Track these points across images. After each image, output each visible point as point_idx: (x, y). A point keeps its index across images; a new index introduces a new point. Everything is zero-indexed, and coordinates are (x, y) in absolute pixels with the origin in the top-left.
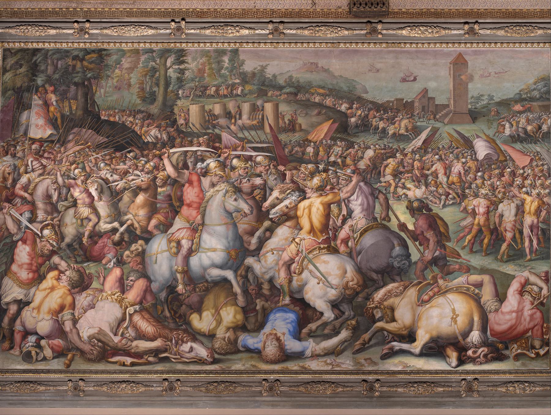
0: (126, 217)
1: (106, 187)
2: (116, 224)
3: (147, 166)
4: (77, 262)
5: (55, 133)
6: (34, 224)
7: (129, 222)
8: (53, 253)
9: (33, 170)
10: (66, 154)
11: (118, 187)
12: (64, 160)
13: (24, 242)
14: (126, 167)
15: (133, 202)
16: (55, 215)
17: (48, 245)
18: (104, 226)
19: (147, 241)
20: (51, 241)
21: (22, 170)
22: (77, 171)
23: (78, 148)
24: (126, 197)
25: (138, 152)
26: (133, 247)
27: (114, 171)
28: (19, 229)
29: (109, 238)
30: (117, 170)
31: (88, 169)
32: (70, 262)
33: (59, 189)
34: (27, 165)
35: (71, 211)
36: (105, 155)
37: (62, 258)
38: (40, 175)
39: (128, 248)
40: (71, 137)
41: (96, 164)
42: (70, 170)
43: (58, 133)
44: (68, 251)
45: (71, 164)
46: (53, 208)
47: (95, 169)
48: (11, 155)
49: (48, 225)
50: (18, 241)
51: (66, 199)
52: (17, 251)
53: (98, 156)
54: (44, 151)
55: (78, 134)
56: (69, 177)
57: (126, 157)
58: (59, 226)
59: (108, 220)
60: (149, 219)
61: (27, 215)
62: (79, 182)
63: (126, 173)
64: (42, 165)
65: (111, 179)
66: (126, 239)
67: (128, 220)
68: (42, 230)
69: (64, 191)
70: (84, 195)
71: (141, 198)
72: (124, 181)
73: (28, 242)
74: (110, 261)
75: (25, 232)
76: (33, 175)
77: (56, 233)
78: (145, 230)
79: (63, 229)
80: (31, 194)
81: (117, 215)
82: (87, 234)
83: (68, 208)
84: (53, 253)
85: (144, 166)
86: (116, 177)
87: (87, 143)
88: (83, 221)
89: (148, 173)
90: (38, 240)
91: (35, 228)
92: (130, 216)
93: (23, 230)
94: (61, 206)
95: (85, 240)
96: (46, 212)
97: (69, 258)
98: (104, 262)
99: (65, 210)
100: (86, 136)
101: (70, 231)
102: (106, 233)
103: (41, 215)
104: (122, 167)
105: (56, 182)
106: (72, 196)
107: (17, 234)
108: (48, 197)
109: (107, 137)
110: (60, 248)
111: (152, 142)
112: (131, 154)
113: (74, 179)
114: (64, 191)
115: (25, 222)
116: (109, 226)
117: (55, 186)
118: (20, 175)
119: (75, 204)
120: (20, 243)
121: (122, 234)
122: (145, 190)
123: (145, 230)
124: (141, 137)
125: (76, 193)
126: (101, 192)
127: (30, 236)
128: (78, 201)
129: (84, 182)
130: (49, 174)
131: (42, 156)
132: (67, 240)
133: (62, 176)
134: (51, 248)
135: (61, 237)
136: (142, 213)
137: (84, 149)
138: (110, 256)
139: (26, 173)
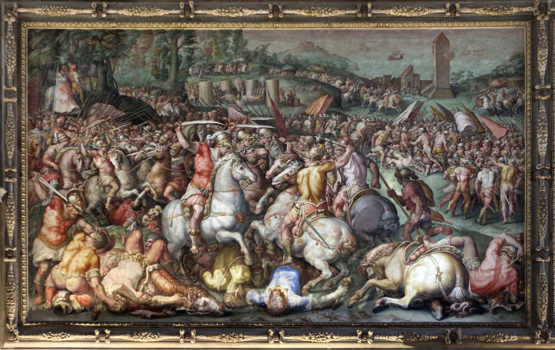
0: (144, 185)
2: (135, 191)
3: (162, 138)
4: (100, 225)
5: (78, 107)
6: (61, 191)
7: (147, 189)
8: (79, 217)
9: (59, 142)
10: (88, 127)
11: (136, 157)
12: (87, 132)
13: (53, 207)
14: (142, 139)
15: (150, 170)
16: (80, 183)
17: (74, 210)
18: (125, 193)
19: (163, 206)
20: (77, 207)
21: (49, 141)
23: (99, 122)
24: (144, 166)
25: (153, 125)
26: (151, 212)
27: (132, 143)
28: (48, 195)
29: (129, 203)
30: (134, 141)
32: (94, 225)
33: (82, 159)
34: (53, 137)
35: (94, 179)
36: (124, 128)
37: (87, 222)
38: (65, 146)
39: (146, 212)
40: (92, 111)
41: (116, 136)
42: (92, 141)
43: (81, 107)
44: (92, 216)
45: (94, 136)
46: (77, 177)
47: (115, 140)
48: (38, 128)
49: (73, 192)
50: (46, 206)
51: (89, 168)
52: (46, 215)
53: (117, 129)
55: (99, 108)
56: (91, 148)
57: (143, 129)
59: (128, 187)
60: (165, 186)
61: (54, 182)
62: (101, 153)
64: (67, 137)
65: (129, 150)
66: (144, 204)
67: (145, 187)
68: (68, 196)
69: (87, 161)
70: (106, 165)
71: (156, 167)
72: (141, 151)
73: (56, 207)
74: (130, 224)
75: (53, 198)
76: (59, 146)
77: (81, 199)
79: (87, 195)
80: (58, 164)
81: (136, 182)
82: (109, 199)
83: (92, 176)
84: (79, 217)
85: (159, 138)
86: (134, 148)
87: (107, 117)
88: (105, 188)
89: (162, 144)
90: (65, 205)
91: (62, 194)
92: (147, 184)
93: (51, 196)
94: (84, 174)
95: (107, 205)
96: (72, 180)
97: (94, 221)
98: (125, 225)
99: (89, 178)
100: (106, 111)
101: (93, 198)
102: (126, 198)
103: (67, 183)
104: (139, 138)
105: (80, 153)
106: (95, 166)
107: (45, 200)
108: (73, 166)
109: (126, 112)
110: (85, 213)
111: (166, 116)
112: (147, 127)
113: (97, 150)
114: (87, 161)
115: (53, 189)
116: (129, 193)
117: (79, 156)
118: (47, 146)
120: (49, 208)
121: (140, 200)
122: (161, 160)
124: (155, 111)
125: (99, 162)
126: (121, 161)
127: (57, 202)
128: (101, 170)
130: (73, 145)
131: (66, 129)
132: (92, 205)
133: (85, 147)
134: (77, 213)
135: (85, 202)
136: (158, 181)
138: (130, 219)
139: (53, 144)
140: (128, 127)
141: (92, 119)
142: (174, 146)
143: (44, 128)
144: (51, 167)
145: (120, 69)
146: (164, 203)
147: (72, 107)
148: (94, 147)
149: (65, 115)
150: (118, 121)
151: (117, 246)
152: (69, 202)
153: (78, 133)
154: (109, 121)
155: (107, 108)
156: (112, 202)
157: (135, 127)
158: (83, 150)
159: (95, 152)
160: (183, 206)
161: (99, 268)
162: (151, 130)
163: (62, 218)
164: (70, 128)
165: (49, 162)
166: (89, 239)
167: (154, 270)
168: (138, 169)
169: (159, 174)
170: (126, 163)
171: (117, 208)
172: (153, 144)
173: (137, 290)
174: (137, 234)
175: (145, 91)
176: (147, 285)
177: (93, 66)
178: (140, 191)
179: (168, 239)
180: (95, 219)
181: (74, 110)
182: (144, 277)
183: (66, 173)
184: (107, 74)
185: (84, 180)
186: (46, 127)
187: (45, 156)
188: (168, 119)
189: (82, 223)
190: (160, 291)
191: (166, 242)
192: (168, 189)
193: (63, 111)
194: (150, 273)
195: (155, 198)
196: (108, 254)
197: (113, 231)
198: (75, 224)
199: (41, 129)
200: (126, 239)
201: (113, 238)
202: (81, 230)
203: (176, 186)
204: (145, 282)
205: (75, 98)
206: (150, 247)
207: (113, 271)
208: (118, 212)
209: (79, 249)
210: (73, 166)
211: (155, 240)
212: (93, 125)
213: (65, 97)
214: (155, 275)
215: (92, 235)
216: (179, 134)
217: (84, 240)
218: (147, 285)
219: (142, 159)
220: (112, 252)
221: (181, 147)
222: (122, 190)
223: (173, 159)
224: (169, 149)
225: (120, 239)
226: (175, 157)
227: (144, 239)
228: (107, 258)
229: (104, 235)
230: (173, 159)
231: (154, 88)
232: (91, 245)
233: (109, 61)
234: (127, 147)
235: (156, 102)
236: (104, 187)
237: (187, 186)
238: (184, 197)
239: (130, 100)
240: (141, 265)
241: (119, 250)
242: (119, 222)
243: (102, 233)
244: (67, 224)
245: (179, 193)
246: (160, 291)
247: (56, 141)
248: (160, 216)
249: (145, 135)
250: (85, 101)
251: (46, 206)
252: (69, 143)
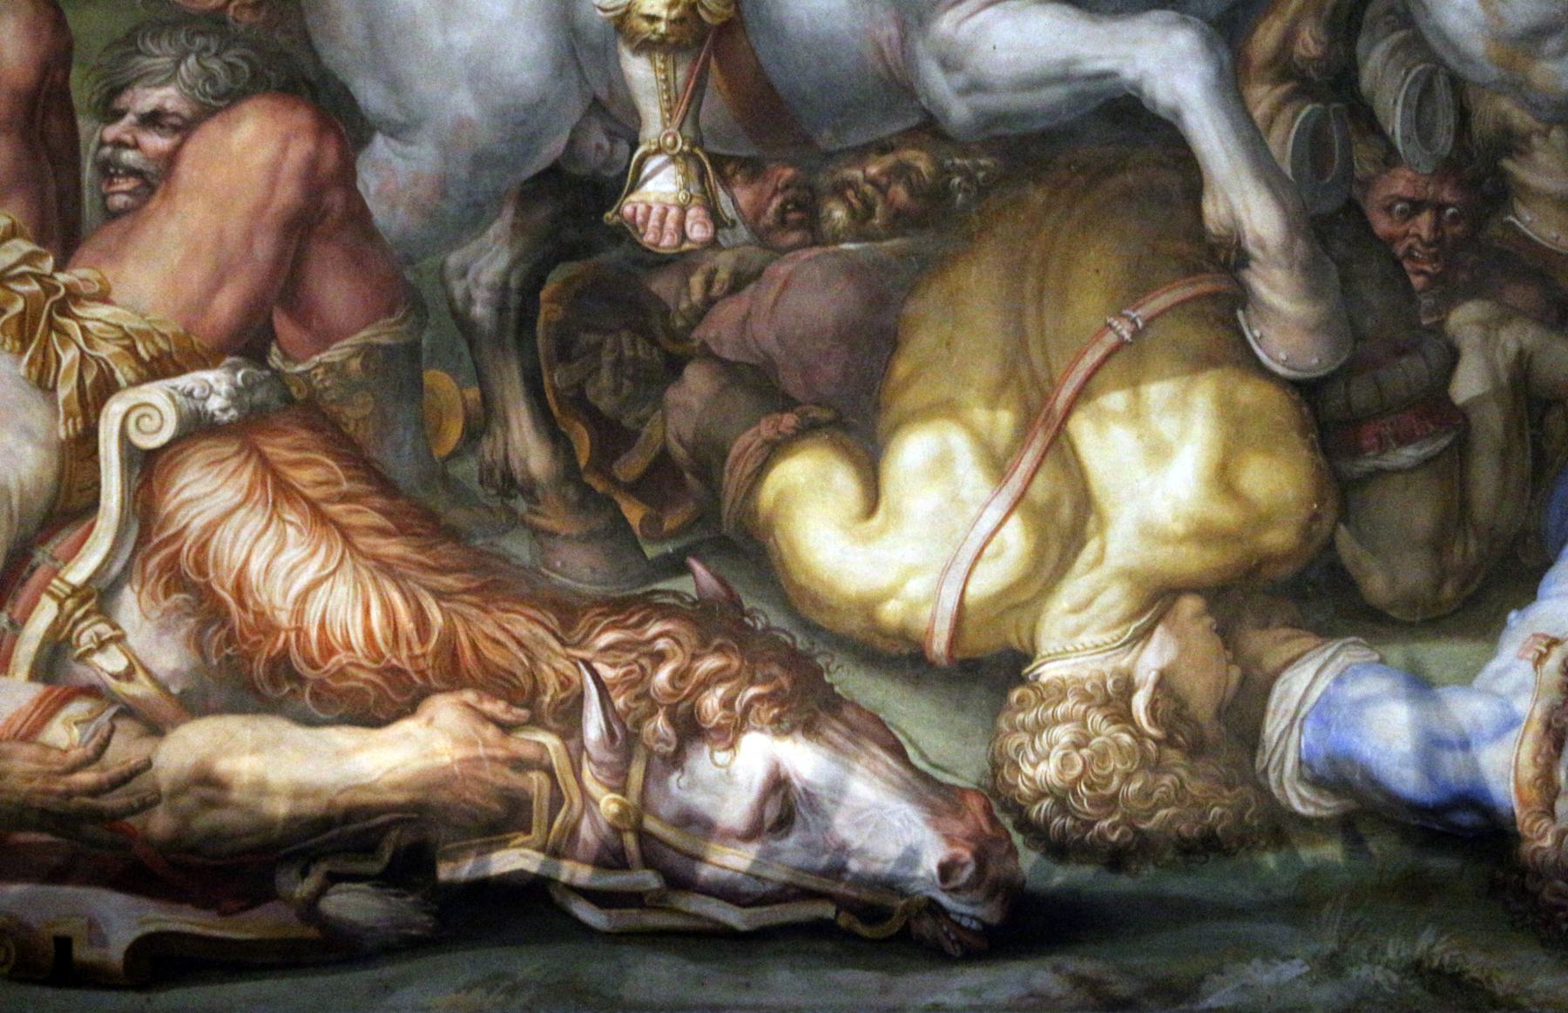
167: (197, 428)
176: (99, 596)
179: (371, 95)
182: (68, 505)
190: (256, 671)
191: (340, 120)
204: (79, 572)
206: (155, 181)
211: (217, 103)
214: (206, 493)
218: (99, 596)
227: (82, 88)
240: (43, 382)
246: (256, 671)
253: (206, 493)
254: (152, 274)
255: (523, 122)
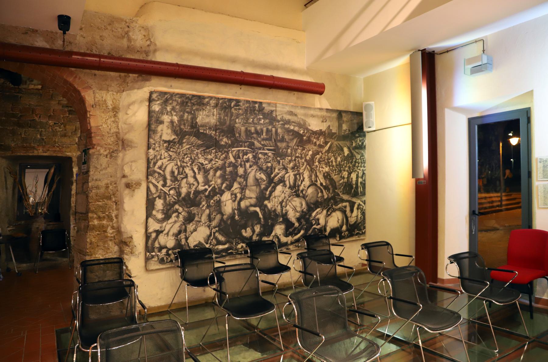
0: (211, 183)
1: (201, 167)
3: (222, 157)
4: (187, 207)
7: (213, 185)
8: (175, 203)
9: (165, 158)
14: (212, 157)
15: (215, 175)
18: (201, 188)
19: (221, 195)
21: (158, 157)
22: (188, 159)
23: (188, 146)
24: (211, 172)
26: (215, 198)
27: (206, 159)
28: (157, 190)
29: (203, 194)
31: (193, 158)
33: (178, 169)
34: (161, 155)
35: (185, 180)
37: (180, 206)
38: (168, 160)
39: (212, 199)
40: (184, 141)
41: (197, 155)
45: (185, 155)
46: (175, 179)
49: (173, 188)
50: (156, 198)
51: (182, 174)
52: (156, 203)
54: (171, 148)
55: (189, 139)
56: (183, 162)
58: (178, 188)
59: (203, 184)
60: (222, 184)
61: (161, 182)
62: (189, 165)
63: (211, 160)
65: (204, 163)
68: (169, 191)
69: (181, 169)
70: (191, 172)
71: (219, 173)
73: (162, 198)
74: (204, 206)
75: (160, 192)
76: (164, 161)
77: (177, 192)
78: (220, 188)
79: (180, 190)
80: (164, 171)
81: (207, 182)
83: (183, 178)
84: (175, 203)
86: (207, 162)
88: (190, 185)
89: (222, 160)
90: (167, 196)
91: (166, 189)
92: (213, 182)
95: (191, 196)
96: (171, 180)
97: (184, 205)
98: (201, 206)
99: (182, 180)
101: (184, 191)
103: (169, 182)
104: (209, 157)
105: (177, 165)
106: (185, 172)
107: (156, 193)
114: (181, 169)
116: (203, 188)
117: (176, 167)
118: (157, 161)
119: (186, 177)
120: (157, 198)
121: (210, 192)
122: (221, 169)
123: (220, 188)
125: (188, 170)
126: (199, 169)
127: (163, 194)
129: (191, 165)
130: (173, 160)
131: (169, 150)
132: (183, 195)
135: (179, 194)
136: (219, 181)
137: (190, 147)
138: (204, 203)
139: (161, 159)
140: (204, 150)
141: (184, 145)
142: (228, 162)
143: (157, 149)
144: (159, 173)
145: (201, 117)
146: (222, 193)
147: (174, 137)
148: (185, 161)
149: (169, 142)
150: (199, 146)
151: (196, 219)
152: (170, 195)
153: (176, 152)
154: (194, 146)
155: (193, 139)
156: (194, 194)
157: (208, 150)
158: (179, 164)
159: (185, 164)
160: (232, 194)
161: (186, 232)
162: (216, 152)
163: (165, 204)
164: (172, 150)
165: (158, 170)
166: (181, 216)
167: (216, 231)
168: (209, 174)
169: (220, 177)
170: (202, 170)
171: (197, 197)
172: (216, 160)
173: (207, 243)
174: (207, 211)
175: (213, 131)
176: (212, 240)
177: (186, 115)
178: (209, 186)
180: (184, 204)
181: (174, 139)
182: (211, 235)
183: (168, 177)
184: (194, 118)
185: (178, 181)
186: (158, 149)
187: (156, 167)
188: (225, 146)
189: (177, 206)
192: (224, 185)
193: (167, 139)
194: (214, 233)
195: (217, 191)
196: (191, 224)
197: (194, 210)
198: (173, 207)
199: (154, 149)
200: (201, 215)
201: (194, 214)
202: (177, 211)
203: (228, 183)
205: (175, 132)
206: (214, 218)
207: (195, 233)
208: (198, 199)
209: (175, 222)
210: (172, 172)
211: (217, 214)
212: (185, 148)
213: (169, 131)
215: (183, 213)
216: (230, 155)
217: (178, 217)
218: (212, 240)
219: (211, 168)
220: (194, 222)
221: (231, 162)
222: (200, 186)
223: (227, 169)
224: (225, 163)
225: (198, 215)
226: (228, 167)
228: (191, 227)
229: (189, 213)
230: (227, 169)
231: (219, 129)
232: (182, 219)
233: (195, 112)
234: (203, 162)
235: (219, 137)
236: (190, 185)
237: (233, 183)
238: (233, 189)
239: (205, 135)
241: (198, 221)
242: (197, 204)
243: (188, 212)
244: (168, 208)
245: (229, 187)
247: (163, 157)
248: (220, 200)
249: (213, 155)
250: (180, 134)
251: (156, 198)
252: (171, 159)
253: (217, 234)
254: (214, 223)
255: (230, 214)
